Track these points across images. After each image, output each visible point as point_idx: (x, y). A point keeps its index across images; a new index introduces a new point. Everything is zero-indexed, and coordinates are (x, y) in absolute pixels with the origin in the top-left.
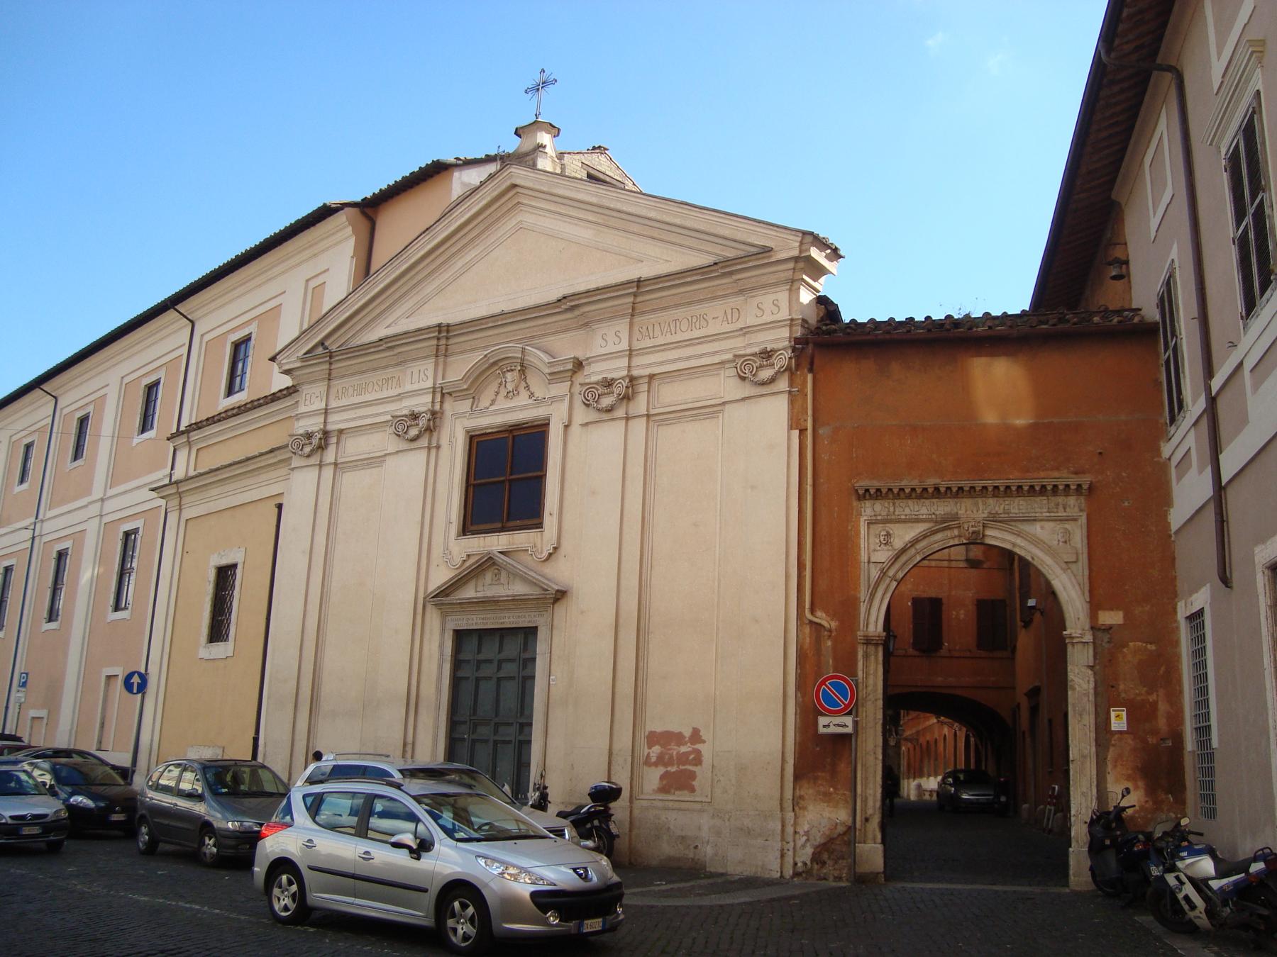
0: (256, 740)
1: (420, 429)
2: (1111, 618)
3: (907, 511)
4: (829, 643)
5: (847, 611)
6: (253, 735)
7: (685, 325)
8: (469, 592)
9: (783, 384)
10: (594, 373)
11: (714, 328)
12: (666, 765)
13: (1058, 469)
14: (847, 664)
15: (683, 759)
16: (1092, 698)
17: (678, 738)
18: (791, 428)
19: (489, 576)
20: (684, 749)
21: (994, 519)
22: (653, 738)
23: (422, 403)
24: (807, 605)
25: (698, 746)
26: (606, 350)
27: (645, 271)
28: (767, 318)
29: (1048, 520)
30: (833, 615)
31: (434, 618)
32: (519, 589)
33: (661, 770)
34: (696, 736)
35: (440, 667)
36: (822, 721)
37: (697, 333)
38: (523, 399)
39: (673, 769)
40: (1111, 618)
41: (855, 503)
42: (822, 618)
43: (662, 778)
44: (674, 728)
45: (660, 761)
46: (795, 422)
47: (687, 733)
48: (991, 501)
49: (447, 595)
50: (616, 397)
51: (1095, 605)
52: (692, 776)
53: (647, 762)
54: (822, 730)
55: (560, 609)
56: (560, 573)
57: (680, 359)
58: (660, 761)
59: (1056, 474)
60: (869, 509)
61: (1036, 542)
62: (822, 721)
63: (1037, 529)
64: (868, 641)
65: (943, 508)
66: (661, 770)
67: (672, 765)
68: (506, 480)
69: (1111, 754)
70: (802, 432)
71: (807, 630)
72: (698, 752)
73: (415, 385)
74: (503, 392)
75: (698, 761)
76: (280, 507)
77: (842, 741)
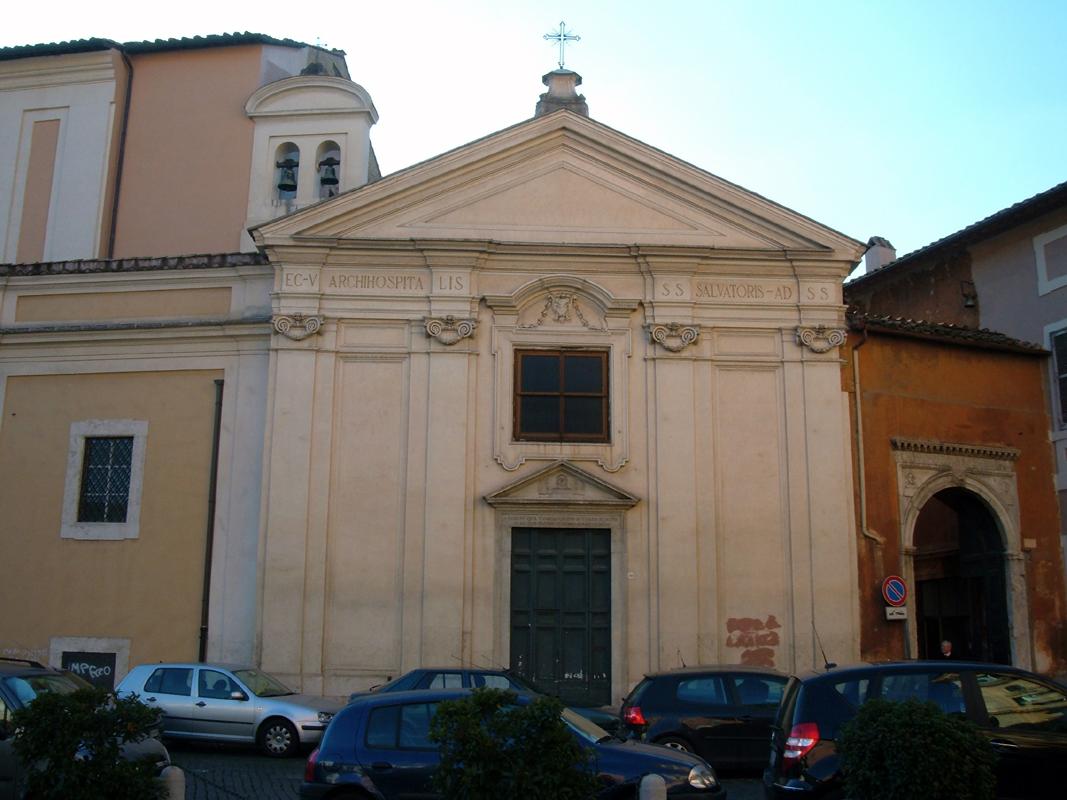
0: (204, 632)
1: (447, 334)
2: (1031, 543)
3: (921, 461)
4: (880, 553)
5: (891, 529)
6: (197, 626)
7: (742, 292)
8: (532, 494)
9: (835, 354)
10: (663, 316)
11: (767, 299)
12: (747, 646)
13: (999, 441)
14: (893, 569)
15: (761, 640)
16: (1025, 595)
17: (757, 624)
18: (843, 390)
19: (553, 481)
20: (761, 633)
21: (971, 472)
22: (732, 624)
23: (461, 310)
24: (865, 525)
25: (775, 630)
26: (674, 296)
27: (719, 242)
28: (817, 301)
29: (998, 475)
30: (882, 532)
31: (488, 515)
32: (591, 494)
33: (743, 650)
34: (772, 622)
35: (498, 560)
36: (889, 610)
37: (752, 300)
38: (575, 325)
39: (754, 649)
40: (1031, 543)
41: (892, 452)
42: (873, 534)
43: (743, 656)
44: (753, 616)
45: (741, 642)
46: (847, 385)
47: (764, 620)
48: (966, 459)
49: (506, 496)
50: (669, 341)
51: (1024, 536)
52: (771, 653)
53: (729, 643)
54: (889, 617)
55: (633, 517)
56: (633, 484)
57: (740, 319)
58: (741, 642)
59: (998, 445)
60: (901, 457)
61: (991, 489)
62: (889, 610)
63: (991, 481)
64: (907, 553)
65: (941, 460)
66: (743, 650)
67: (752, 645)
68: (561, 396)
69: (1036, 632)
70: (853, 394)
71: (863, 542)
72: (775, 636)
73: (453, 290)
74: (551, 316)
75: (775, 641)
76: (220, 384)
77: (901, 623)
